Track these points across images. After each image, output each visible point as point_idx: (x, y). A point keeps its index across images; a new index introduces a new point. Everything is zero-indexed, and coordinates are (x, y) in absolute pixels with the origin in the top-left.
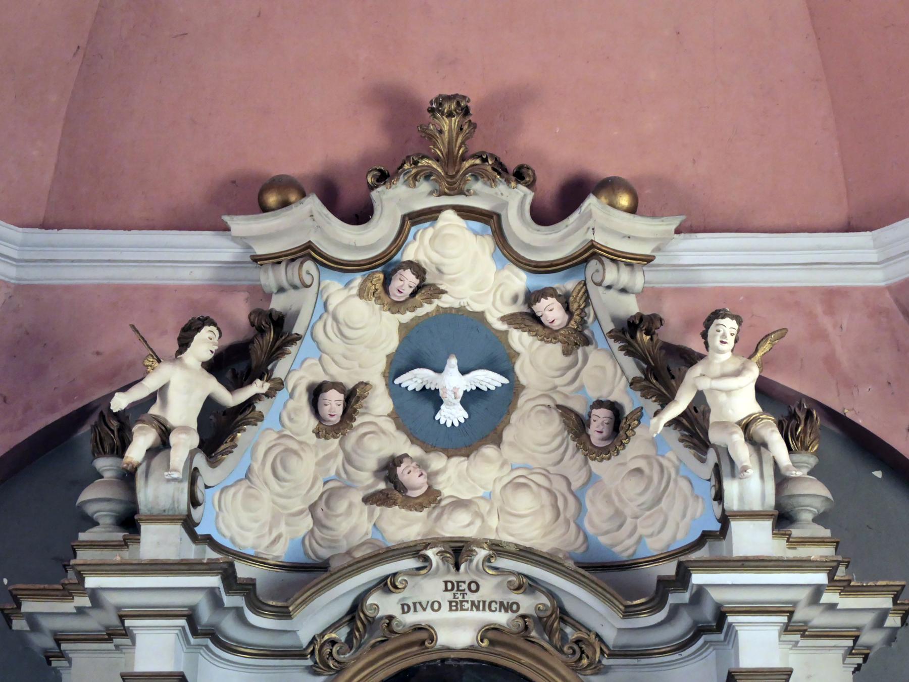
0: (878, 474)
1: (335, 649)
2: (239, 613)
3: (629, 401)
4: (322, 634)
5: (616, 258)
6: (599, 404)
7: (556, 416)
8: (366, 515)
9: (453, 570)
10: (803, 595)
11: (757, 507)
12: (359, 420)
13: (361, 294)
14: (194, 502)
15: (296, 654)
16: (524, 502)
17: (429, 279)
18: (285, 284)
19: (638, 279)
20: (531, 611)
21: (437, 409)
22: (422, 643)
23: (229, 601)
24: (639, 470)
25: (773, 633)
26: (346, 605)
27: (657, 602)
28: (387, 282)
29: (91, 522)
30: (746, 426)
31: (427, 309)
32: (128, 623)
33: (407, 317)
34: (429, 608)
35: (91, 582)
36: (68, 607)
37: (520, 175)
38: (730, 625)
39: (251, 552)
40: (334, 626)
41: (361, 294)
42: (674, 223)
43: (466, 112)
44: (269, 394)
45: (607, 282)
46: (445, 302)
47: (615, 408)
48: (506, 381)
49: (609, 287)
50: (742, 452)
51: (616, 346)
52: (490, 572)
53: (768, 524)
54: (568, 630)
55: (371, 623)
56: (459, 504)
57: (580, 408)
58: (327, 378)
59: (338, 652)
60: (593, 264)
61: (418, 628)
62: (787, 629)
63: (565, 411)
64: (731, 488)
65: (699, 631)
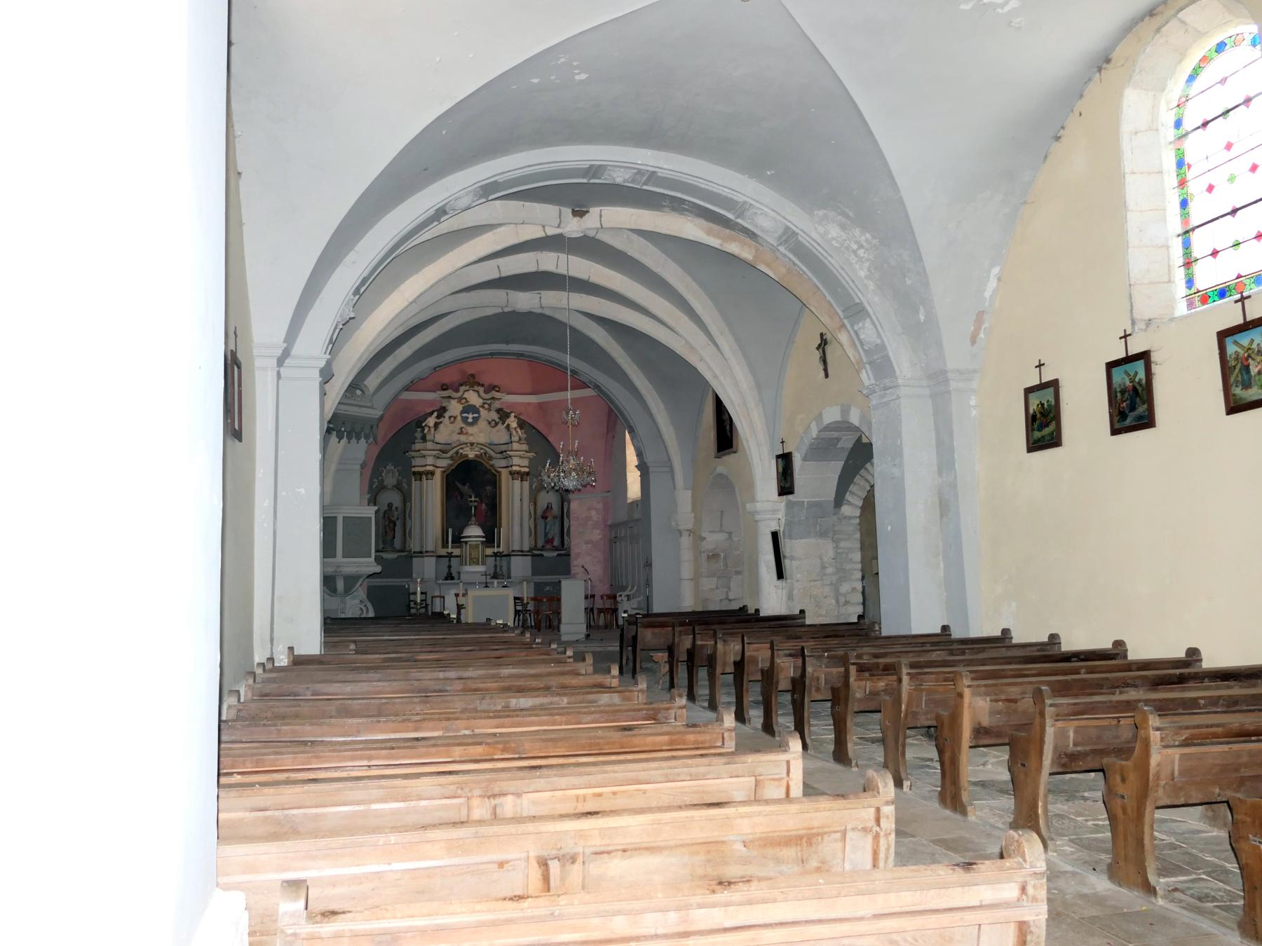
16: (481, 434)
30: (515, 428)
37: (483, 385)
56: (471, 435)
57: (490, 420)
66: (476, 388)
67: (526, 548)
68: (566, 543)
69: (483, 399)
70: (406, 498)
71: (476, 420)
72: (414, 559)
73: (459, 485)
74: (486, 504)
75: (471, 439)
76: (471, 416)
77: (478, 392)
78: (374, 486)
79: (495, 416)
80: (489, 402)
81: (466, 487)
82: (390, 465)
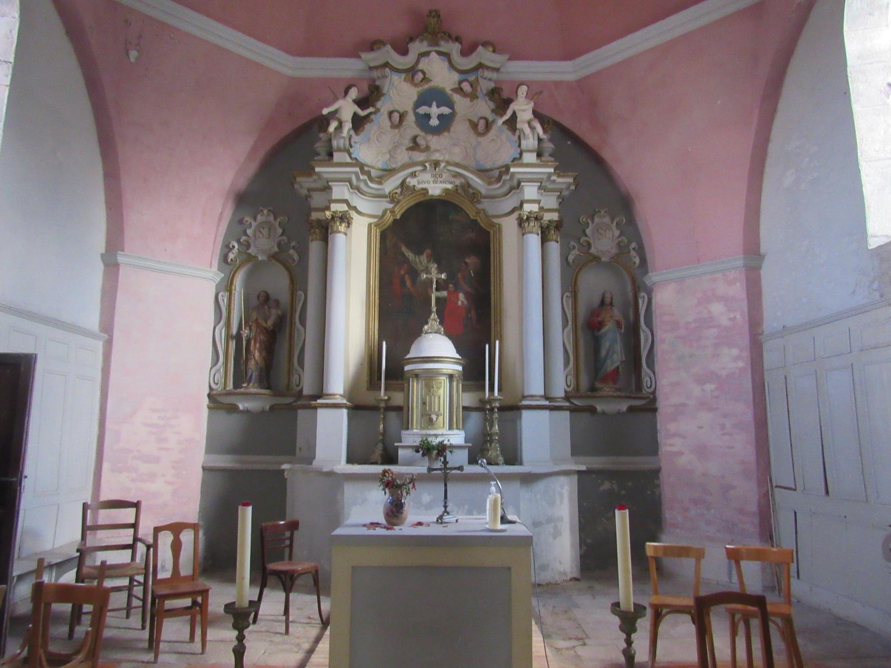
0: (569, 143)
1: (397, 196)
2: (365, 181)
3: (491, 117)
4: (393, 191)
5: (488, 68)
6: (481, 118)
7: (467, 123)
8: (407, 154)
9: (434, 170)
10: (545, 177)
11: (531, 149)
12: (404, 123)
13: (405, 80)
14: (351, 146)
15: (385, 196)
16: (457, 150)
17: (427, 76)
18: (380, 76)
19: (494, 76)
20: (459, 185)
21: (429, 120)
22: (424, 194)
23: (362, 177)
24: (493, 140)
25: (536, 189)
26: (400, 181)
27: (499, 179)
28: (413, 78)
29: (318, 154)
31: (426, 86)
32: (330, 183)
33: (420, 89)
34: (426, 183)
35: (317, 169)
36: (311, 179)
37: (457, 39)
38: (522, 186)
39: (370, 165)
40: (397, 188)
41: (405, 80)
42: (507, 57)
43: (439, 16)
44: (375, 113)
45: (485, 76)
46: (432, 84)
47: (486, 119)
48: (451, 111)
49: (485, 78)
50: (527, 130)
51: (487, 98)
52: (446, 171)
53: (535, 154)
54: (471, 190)
55: (408, 187)
57: (475, 120)
58: (395, 109)
59: (398, 196)
60: (480, 70)
61: (423, 189)
62: (540, 188)
63: (470, 121)
64: (523, 143)
65: (511, 189)
66: (445, 46)
67: (559, 391)
68: (646, 380)
69: (461, 72)
70: (297, 281)
71: (446, 122)
72: (300, 412)
73: (410, 255)
74: (467, 295)
75: (436, 156)
76: (435, 110)
77: (446, 55)
78: (231, 256)
79: (484, 108)
80: (472, 78)
81: (424, 258)
82: (265, 212)
